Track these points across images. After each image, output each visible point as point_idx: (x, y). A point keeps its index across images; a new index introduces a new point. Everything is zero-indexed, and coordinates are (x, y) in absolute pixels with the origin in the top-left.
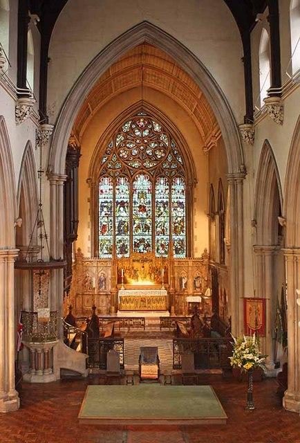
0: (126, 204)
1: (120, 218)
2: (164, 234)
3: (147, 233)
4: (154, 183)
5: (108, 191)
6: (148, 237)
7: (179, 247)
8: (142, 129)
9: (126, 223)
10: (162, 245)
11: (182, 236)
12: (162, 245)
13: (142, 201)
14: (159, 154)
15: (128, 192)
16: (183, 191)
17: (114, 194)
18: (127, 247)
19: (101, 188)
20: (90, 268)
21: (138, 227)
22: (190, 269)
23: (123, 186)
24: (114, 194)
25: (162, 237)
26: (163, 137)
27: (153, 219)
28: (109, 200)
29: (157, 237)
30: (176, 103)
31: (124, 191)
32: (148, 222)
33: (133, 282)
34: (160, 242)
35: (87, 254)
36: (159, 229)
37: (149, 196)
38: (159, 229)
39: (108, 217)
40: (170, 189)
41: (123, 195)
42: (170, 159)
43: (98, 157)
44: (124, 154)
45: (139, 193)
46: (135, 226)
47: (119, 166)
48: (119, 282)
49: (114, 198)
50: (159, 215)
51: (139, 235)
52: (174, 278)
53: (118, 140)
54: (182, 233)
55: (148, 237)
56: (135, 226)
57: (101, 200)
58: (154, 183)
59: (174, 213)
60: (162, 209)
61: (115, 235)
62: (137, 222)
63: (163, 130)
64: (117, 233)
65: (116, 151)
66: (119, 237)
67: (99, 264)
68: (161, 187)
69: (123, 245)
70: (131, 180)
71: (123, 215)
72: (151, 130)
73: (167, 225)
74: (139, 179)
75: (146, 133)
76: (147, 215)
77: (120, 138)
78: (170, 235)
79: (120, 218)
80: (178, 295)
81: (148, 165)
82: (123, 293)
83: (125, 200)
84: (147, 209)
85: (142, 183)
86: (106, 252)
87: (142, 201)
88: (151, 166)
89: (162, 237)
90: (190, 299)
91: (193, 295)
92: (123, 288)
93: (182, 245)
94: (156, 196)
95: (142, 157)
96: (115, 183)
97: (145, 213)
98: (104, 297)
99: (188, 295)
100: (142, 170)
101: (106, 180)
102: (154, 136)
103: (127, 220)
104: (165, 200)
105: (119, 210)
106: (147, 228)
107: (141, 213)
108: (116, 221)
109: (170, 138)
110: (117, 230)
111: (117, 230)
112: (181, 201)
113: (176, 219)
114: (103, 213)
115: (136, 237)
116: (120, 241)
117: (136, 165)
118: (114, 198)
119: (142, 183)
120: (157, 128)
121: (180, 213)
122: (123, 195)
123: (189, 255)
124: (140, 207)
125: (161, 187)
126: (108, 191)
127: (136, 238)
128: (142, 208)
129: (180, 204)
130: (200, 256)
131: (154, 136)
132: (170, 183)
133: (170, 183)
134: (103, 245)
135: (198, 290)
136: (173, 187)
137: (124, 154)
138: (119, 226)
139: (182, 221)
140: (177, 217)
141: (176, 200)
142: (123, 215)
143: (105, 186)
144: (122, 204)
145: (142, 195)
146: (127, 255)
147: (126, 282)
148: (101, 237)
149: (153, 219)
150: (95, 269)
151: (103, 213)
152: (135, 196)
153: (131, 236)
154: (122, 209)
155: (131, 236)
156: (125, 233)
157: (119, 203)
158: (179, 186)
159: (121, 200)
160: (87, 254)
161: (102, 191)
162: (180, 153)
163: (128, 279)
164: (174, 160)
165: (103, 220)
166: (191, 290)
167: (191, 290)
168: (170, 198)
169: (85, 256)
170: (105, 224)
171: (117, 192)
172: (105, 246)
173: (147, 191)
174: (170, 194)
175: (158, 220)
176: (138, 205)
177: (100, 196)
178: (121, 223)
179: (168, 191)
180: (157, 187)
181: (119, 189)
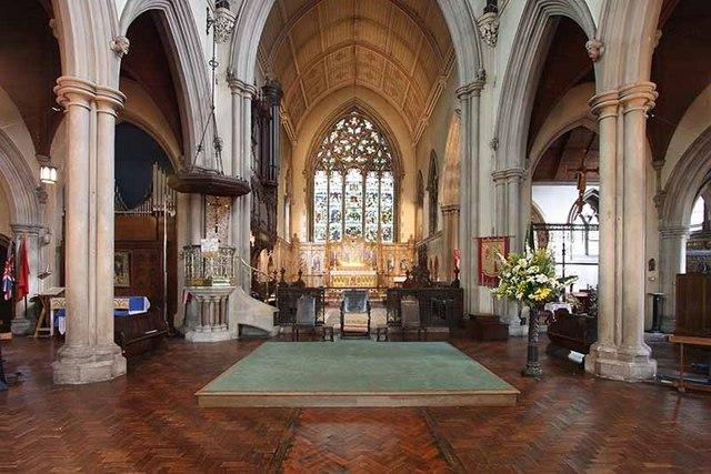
4: (365, 176)
8: (355, 127)
11: (390, 224)
14: (370, 150)
19: (316, 180)
23: (337, 177)
26: (373, 134)
27: (364, 209)
30: (387, 101)
32: (359, 211)
33: (344, 264)
35: (303, 238)
37: (361, 187)
41: (336, 187)
42: (379, 154)
43: (314, 152)
47: (332, 160)
48: (332, 264)
57: (316, 192)
58: (365, 176)
59: (382, 204)
63: (375, 128)
65: (330, 146)
70: (344, 173)
71: (336, 205)
72: (363, 128)
73: (376, 214)
75: (358, 130)
77: (334, 135)
78: (379, 224)
81: (359, 159)
90: (397, 279)
93: (389, 232)
95: (355, 153)
96: (329, 174)
98: (317, 278)
100: (354, 165)
102: (366, 134)
103: (340, 210)
109: (381, 135)
114: (318, 204)
117: (349, 159)
119: (354, 176)
120: (369, 126)
121: (389, 203)
122: (336, 187)
123: (396, 240)
128: (354, 199)
131: (366, 134)
132: (380, 175)
133: (380, 175)
138: (333, 215)
139: (390, 211)
142: (336, 205)
143: (320, 177)
144: (336, 195)
145: (354, 186)
146: (339, 241)
147: (337, 265)
148: (316, 224)
149: (364, 209)
151: (318, 204)
152: (347, 187)
153: (343, 224)
155: (343, 224)
156: (338, 220)
158: (388, 179)
160: (303, 238)
162: (390, 150)
163: (340, 261)
164: (384, 156)
165: (317, 209)
166: (397, 271)
167: (397, 271)
175: (367, 209)
178: (334, 212)
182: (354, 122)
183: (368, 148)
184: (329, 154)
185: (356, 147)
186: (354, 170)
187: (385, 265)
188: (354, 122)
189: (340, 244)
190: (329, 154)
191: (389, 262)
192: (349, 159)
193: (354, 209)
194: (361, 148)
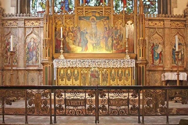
20: (13, 31)
22: (167, 31)
33: (78, 50)
48: (57, 51)
52: (144, 40)
67: (28, 24)
80: (149, 71)
82: (61, 62)
86: (40, 9)
90: (171, 76)
91: (172, 71)
92: (62, 57)
99: (164, 71)
130: (181, 13)
135: (180, 64)
150: (20, 31)
163: (72, 46)
169: (7, 12)
187: (149, 54)
189: (71, 17)
191: (154, 47)
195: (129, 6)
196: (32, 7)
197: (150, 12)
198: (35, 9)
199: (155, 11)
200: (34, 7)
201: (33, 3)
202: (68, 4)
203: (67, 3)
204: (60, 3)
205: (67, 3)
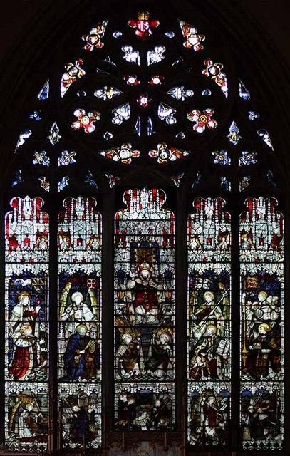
0: (90, 283)
1: (71, 328)
2: (215, 378)
3: (159, 373)
5: (33, 238)
6: (162, 386)
7: (262, 417)
9: (90, 344)
10: (209, 412)
12: (209, 412)
13: (145, 273)
14: (201, 122)
15: (96, 244)
16: (276, 239)
17: (54, 249)
18: (94, 420)
19: (13, 228)
21: (132, 355)
23: (82, 223)
24: (54, 249)
25: (210, 385)
27: (180, 328)
28: (36, 269)
29: (193, 387)
31: (87, 239)
34: (202, 401)
36: (199, 361)
38: (199, 361)
39: (32, 324)
40: (235, 233)
42: (233, 133)
44: (85, 121)
45: (133, 245)
46: (122, 350)
49: (53, 261)
50: (200, 317)
51: (134, 379)
53: (65, 77)
54: (272, 374)
55: (162, 386)
56: (122, 350)
57: (10, 270)
60: (209, 297)
61: (54, 383)
62: (127, 338)
64: (60, 373)
65: (60, 110)
66: (67, 388)
68: (207, 225)
69: (83, 412)
70: (108, 205)
73: (225, 347)
74: (133, 201)
75: (156, 56)
76: (160, 316)
78: (236, 382)
79: (71, 328)
81: (163, 154)
83: (88, 269)
84: (161, 298)
85: (144, 211)
86: (28, 433)
87: (145, 273)
88: (173, 158)
89: (210, 385)
94: (191, 255)
97: (155, 311)
101: (27, 206)
104: (218, 268)
105: (70, 302)
106: (159, 357)
107: (140, 310)
108: (61, 334)
110: (61, 363)
111: (61, 363)
112: (271, 269)
113: (256, 329)
114: (18, 310)
115: (126, 385)
116: (72, 400)
118: (53, 261)
119: (144, 211)
124: (138, 290)
125: (207, 225)
126: (33, 238)
127: (125, 392)
128: (145, 295)
129: (267, 282)
132: (235, 211)
133: (235, 211)
134: (18, 413)
136: (245, 226)
137: (84, 121)
138: (70, 353)
140: (258, 321)
141: (253, 269)
144: (80, 281)
145: (145, 251)
152: (124, 255)
153: (108, 386)
154: (78, 297)
155: (108, 386)
156: (88, 374)
157: (70, 279)
159: (77, 267)
161: (13, 240)
168: (235, 262)
170: (24, 344)
171: (62, 242)
172: (24, 415)
173: (161, 241)
174: (235, 249)
176: (133, 284)
177: (9, 256)
178: (76, 342)
179: (226, 241)
180: (196, 228)
181: (67, 234)
182: (143, 25)
183: (195, 117)
184: (55, 137)
185: (151, 110)
186: (145, 195)
188: (143, 25)
190: (55, 137)
192: (125, 154)
193: (145, 330)
194: (165, 113)
195: (222, 425)
196: (9, 427)
197: (267, 435)
198: (16, 432)
199: (279, 433)
200: (13, 429)
201: (9, 418)
202: (88, 424)
203: (86, 421)
204: (69, 421)
205: (86, 421)
